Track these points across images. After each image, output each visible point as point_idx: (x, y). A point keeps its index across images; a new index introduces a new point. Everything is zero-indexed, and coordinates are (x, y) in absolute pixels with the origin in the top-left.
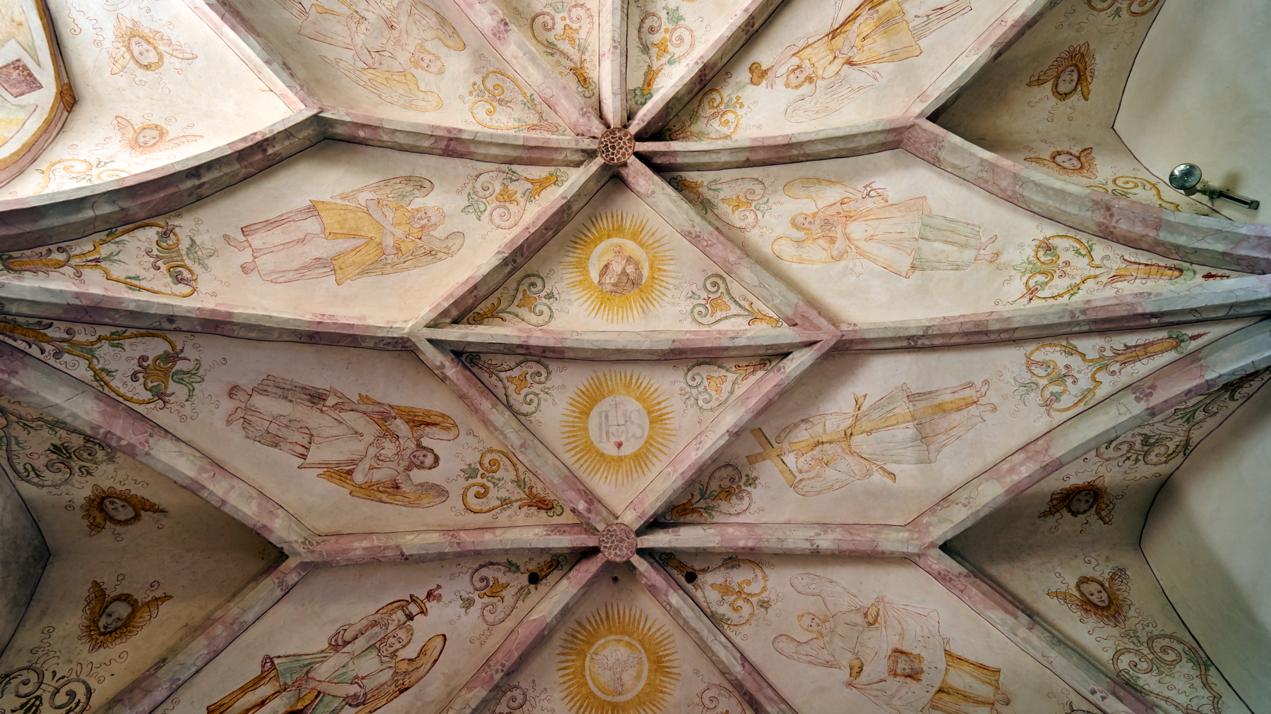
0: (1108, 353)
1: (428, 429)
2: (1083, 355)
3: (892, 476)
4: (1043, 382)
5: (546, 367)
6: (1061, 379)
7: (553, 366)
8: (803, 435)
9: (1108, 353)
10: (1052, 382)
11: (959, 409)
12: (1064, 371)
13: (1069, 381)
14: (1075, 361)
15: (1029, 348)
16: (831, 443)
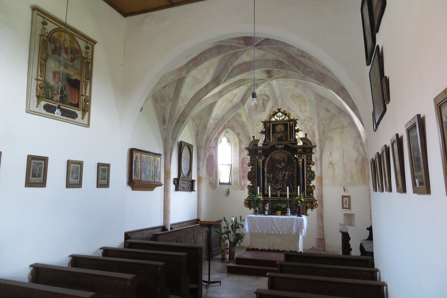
0: (181, 110)
1: (301, 55)
2: (183, 106)
3: (197, 71)
4: (185, 99)
5: (276, 59)
6: (183, 102)
7: (275, 59)
8: (216, 65)
9: (181, 110)
10: (184, 100)
11: (193, 85)
12: (183, 103)
13: (182, 102)
14: (183, 105)
15: (189, 100)
16: (211, 67)
